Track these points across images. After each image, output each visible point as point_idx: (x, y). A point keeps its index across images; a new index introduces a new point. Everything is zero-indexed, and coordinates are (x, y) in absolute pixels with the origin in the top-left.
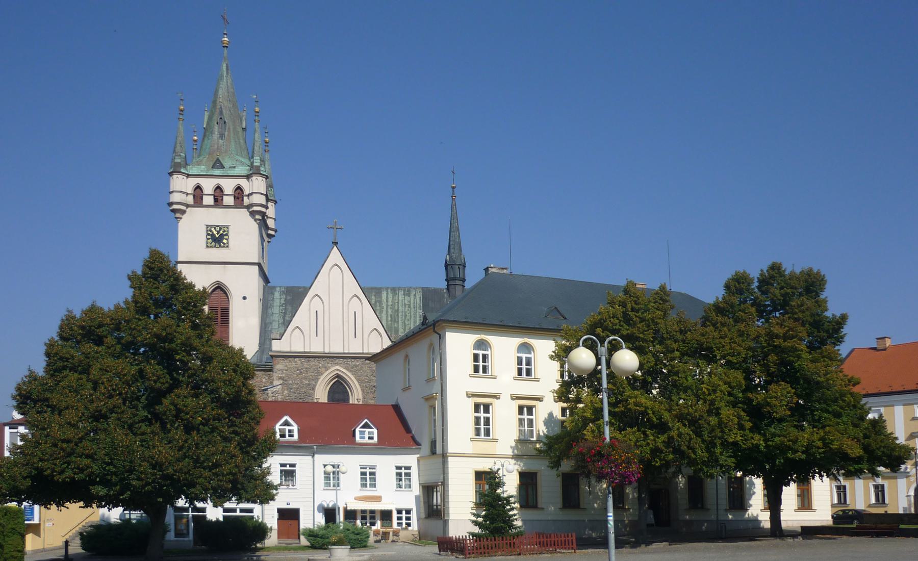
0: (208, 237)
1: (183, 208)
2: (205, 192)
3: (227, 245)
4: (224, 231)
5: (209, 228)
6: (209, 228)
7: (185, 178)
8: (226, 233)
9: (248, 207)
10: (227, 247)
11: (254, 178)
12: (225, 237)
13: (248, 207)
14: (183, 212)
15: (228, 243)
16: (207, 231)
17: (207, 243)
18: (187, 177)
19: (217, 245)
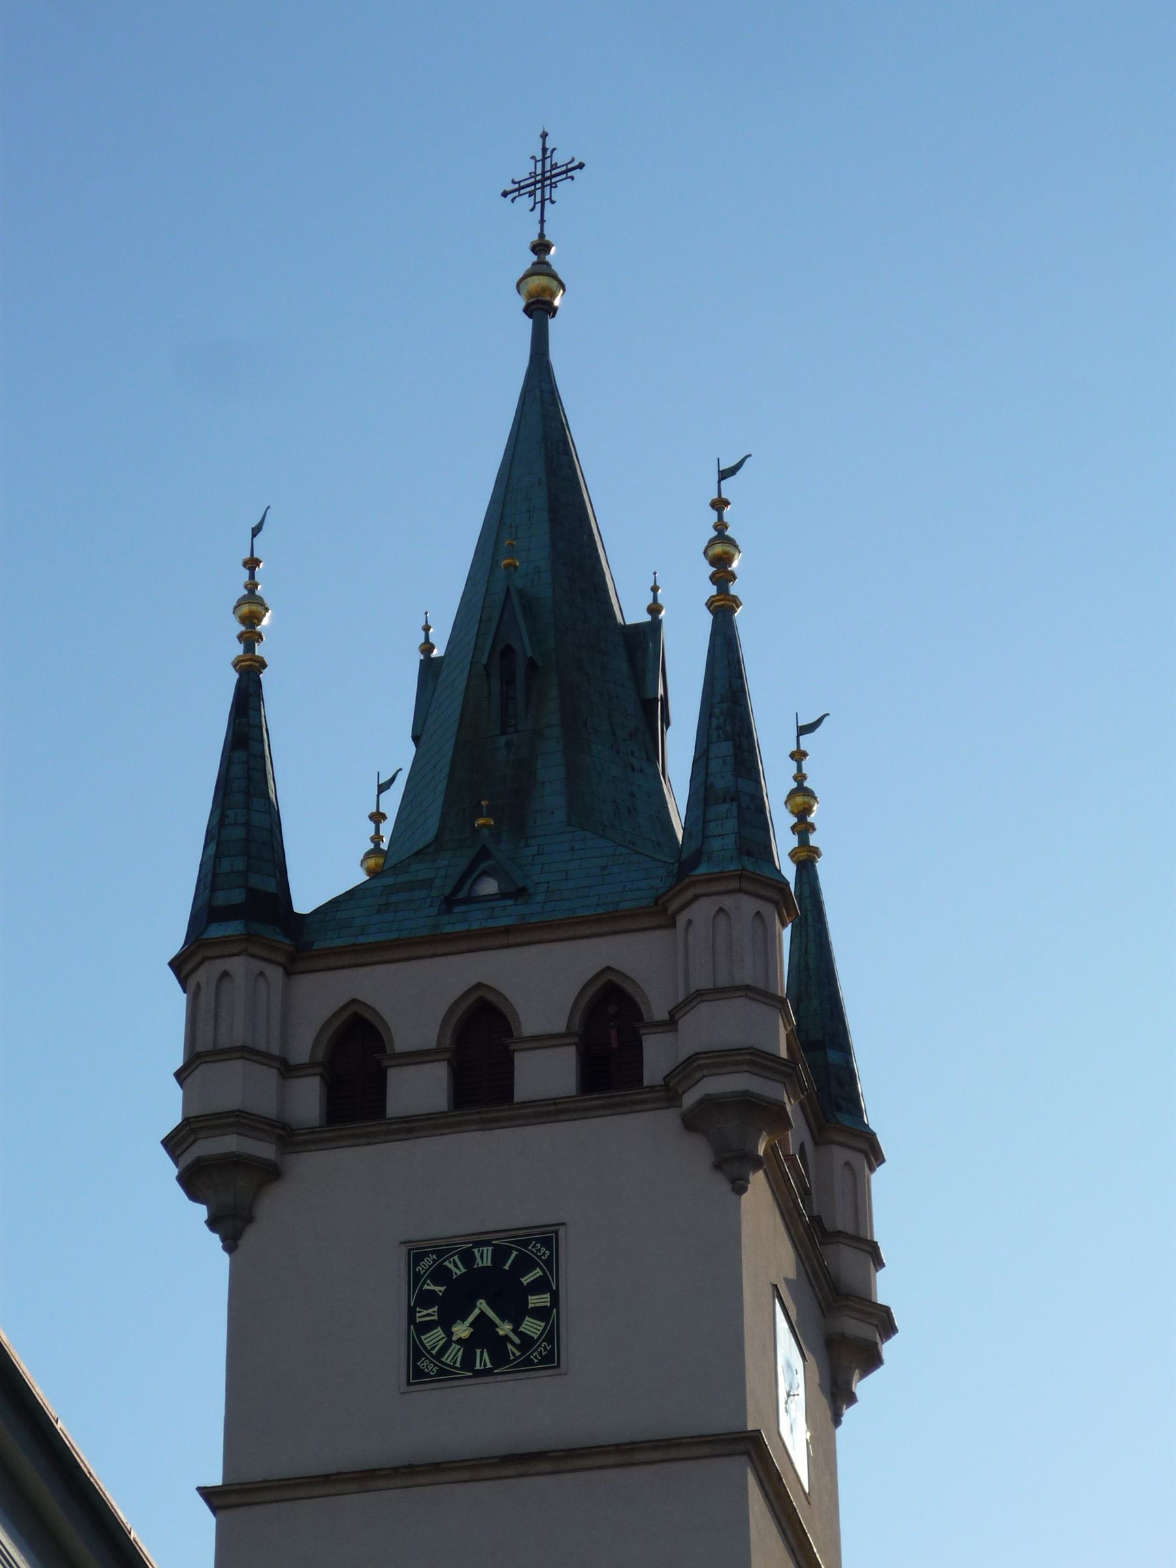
0: (422, 1315)
1: (265, 1150)
2: (404, 1038)
4: (525, 1263)
5: (427, 1263)
6: (427, 1263)
7: (275, 974)
8: (537, 1273)
9: (668, 1093)
10: (551, 1359)
11: (702, 911)
12: (535, 1301)
13: (668, 1093)
14: (272, 1173)
15: (551, 1335)
16: (418, 1276)
17: (416, 1352)
18: (289, 973)
19: (483, 1359)
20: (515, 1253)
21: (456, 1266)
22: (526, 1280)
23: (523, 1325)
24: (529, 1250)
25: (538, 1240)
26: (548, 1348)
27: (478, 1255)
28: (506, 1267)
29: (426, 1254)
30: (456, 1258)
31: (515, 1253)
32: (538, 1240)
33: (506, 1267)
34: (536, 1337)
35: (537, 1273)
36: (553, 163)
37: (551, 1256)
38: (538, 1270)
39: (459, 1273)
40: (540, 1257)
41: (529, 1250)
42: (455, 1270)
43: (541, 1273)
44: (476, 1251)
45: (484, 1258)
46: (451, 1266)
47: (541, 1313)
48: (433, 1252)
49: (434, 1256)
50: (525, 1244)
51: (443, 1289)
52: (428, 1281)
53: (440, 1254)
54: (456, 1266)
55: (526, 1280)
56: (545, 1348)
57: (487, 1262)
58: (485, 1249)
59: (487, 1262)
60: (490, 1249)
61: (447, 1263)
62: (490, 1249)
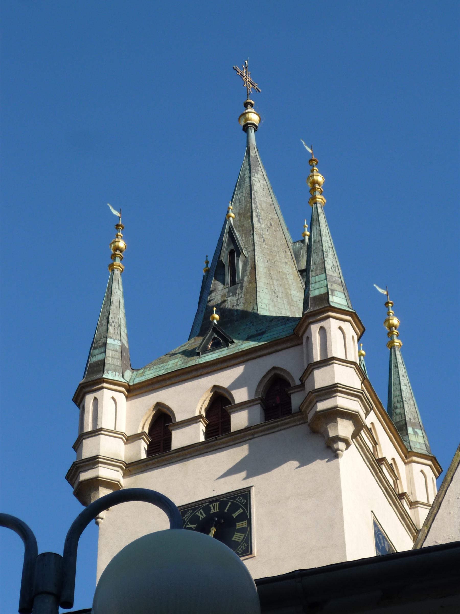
3: (243, 546)
4: (235, 508)
8: (241, 511)
20: (230, 503)
21: (201, 514)
22: (235, 515)
23: (234, 537)
24: (237, 501)
25: (240, 496)
26: (246, 546)
27: (212, 508)
28: (226, 511)
29: (188, 511)
30: (201, 510)
31: (230, 503)
32: (240, 496)
33: (226, 511)
34: (240, 541)
35: (241, 511)
36: (314, 293)
37: (247, 502)
38: (241, 509)
39: (203, 517)
40: (242, 504)
41: (237, 501)
42: (201, 516)
43: (242, 511)
44: (211, 505)
45: (215, 508)
46: (199, 515)
47: (243, 530)
48: (190, 510)
49: (191, 511)
50: (234, 498)
51: (195, 526)
52: (188, 523)
53: (194, 510)
54: (201, 514)
55: (235, 515)
56: (244, 546)
57: (217, 510)
58: (215, 504)
59: (217, 510)
60: (218, 503)
61: (197, 514)
62: (218, 503)
